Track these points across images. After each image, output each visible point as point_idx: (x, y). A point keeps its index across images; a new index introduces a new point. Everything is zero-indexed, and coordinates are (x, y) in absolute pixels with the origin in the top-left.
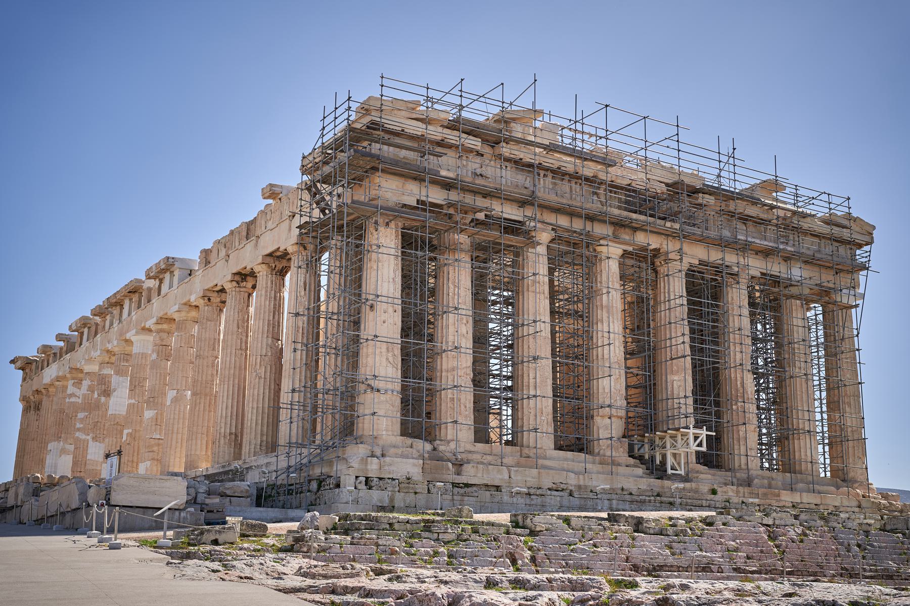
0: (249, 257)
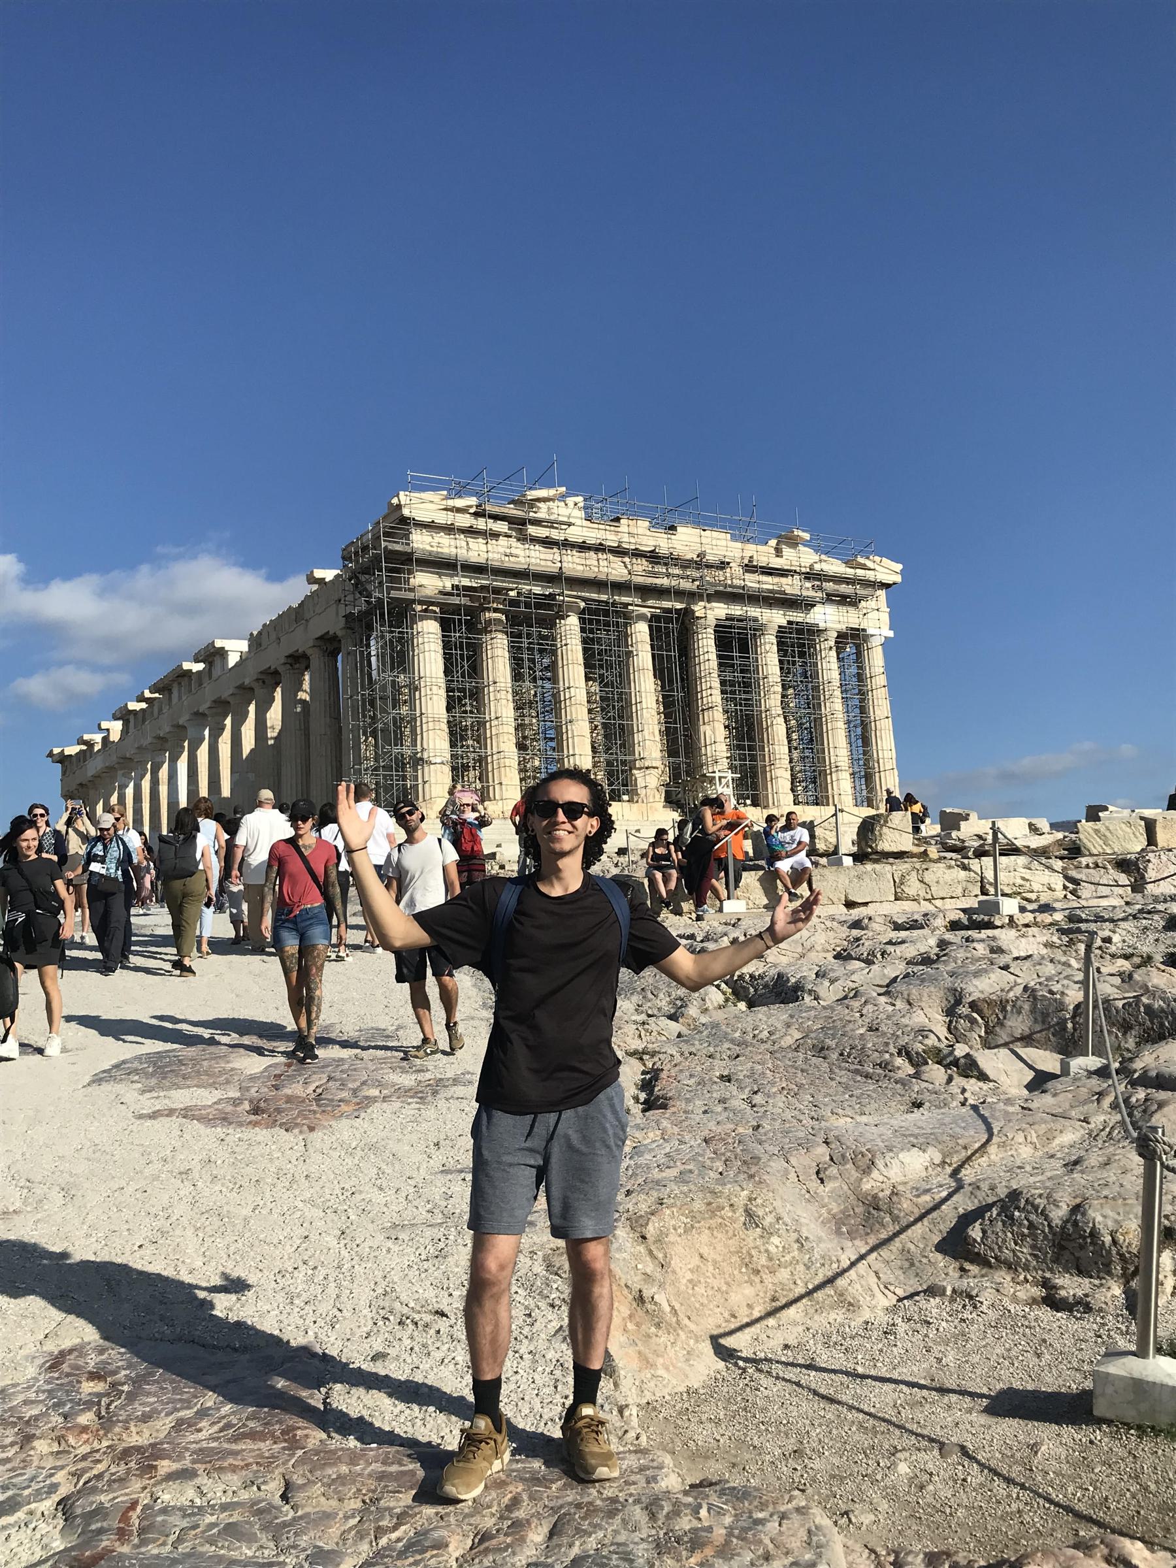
0: (302, 640)
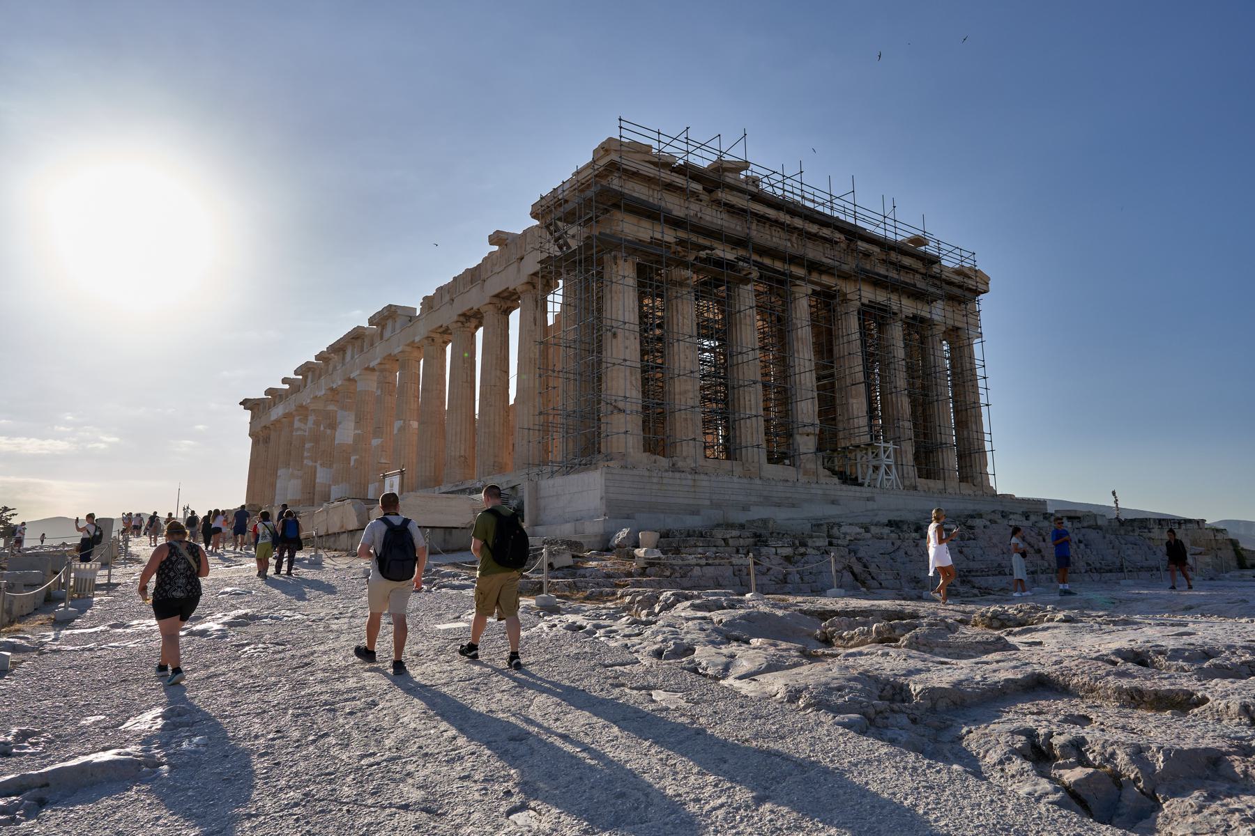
0: (476, 299)
